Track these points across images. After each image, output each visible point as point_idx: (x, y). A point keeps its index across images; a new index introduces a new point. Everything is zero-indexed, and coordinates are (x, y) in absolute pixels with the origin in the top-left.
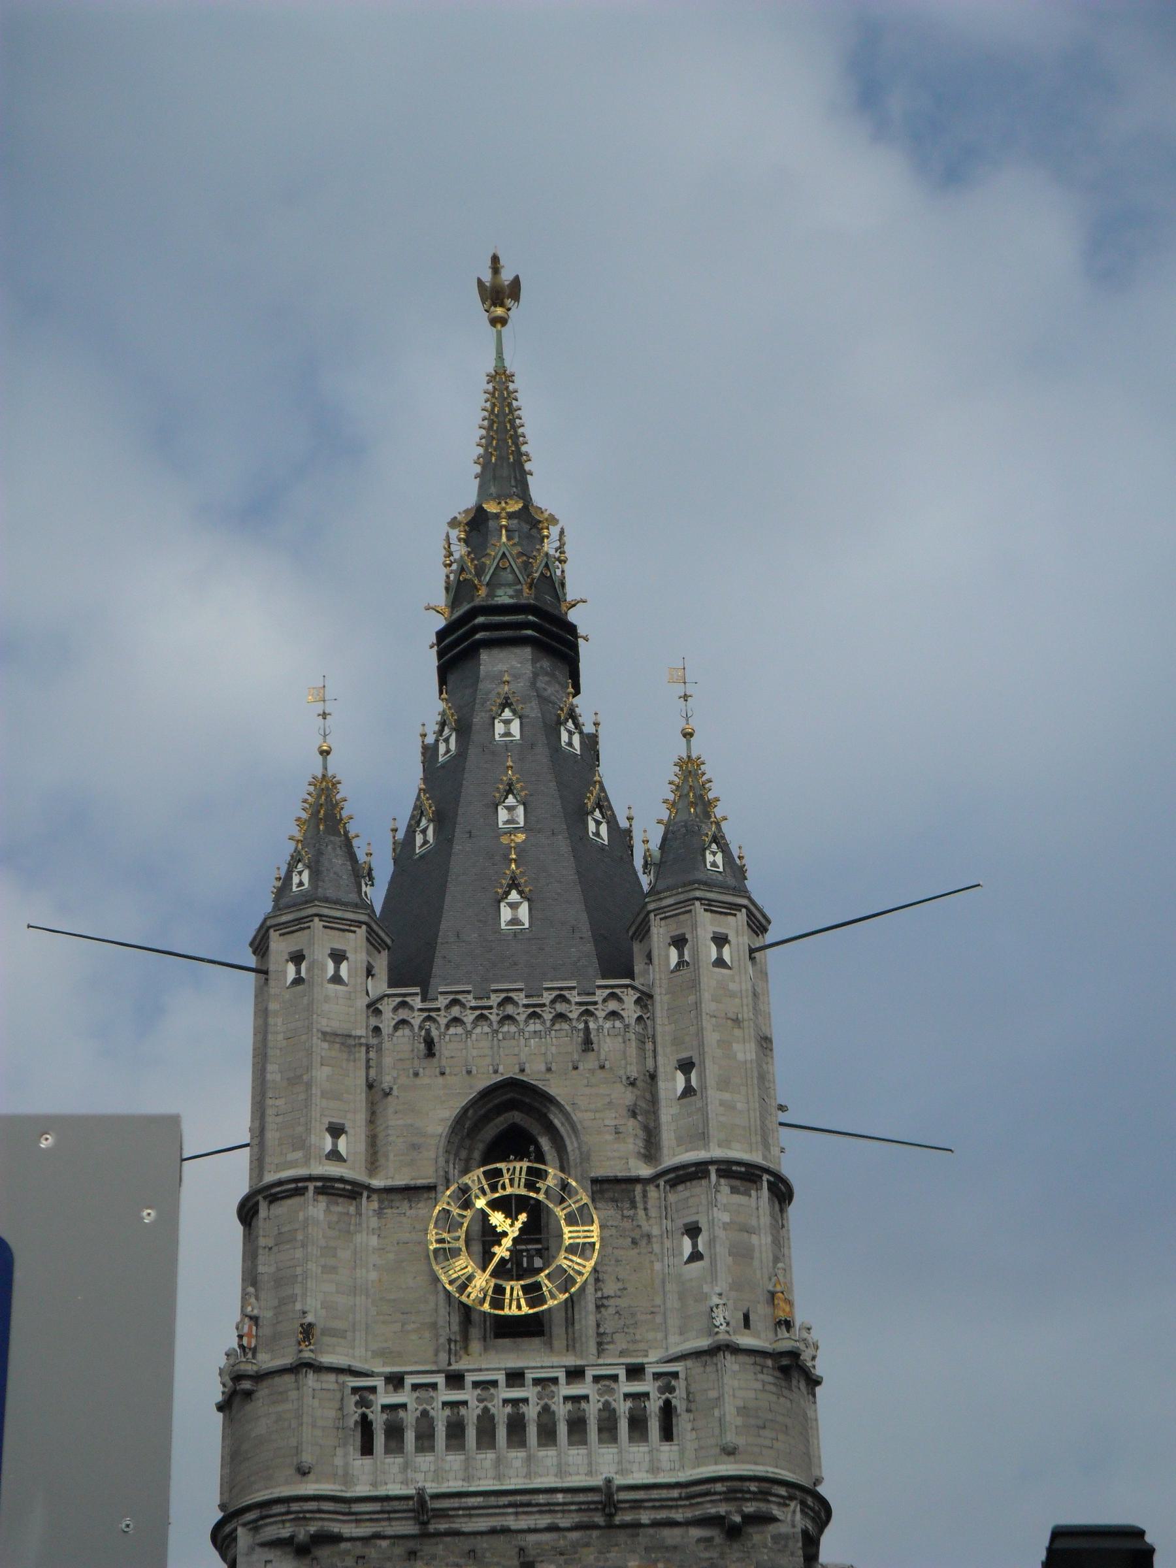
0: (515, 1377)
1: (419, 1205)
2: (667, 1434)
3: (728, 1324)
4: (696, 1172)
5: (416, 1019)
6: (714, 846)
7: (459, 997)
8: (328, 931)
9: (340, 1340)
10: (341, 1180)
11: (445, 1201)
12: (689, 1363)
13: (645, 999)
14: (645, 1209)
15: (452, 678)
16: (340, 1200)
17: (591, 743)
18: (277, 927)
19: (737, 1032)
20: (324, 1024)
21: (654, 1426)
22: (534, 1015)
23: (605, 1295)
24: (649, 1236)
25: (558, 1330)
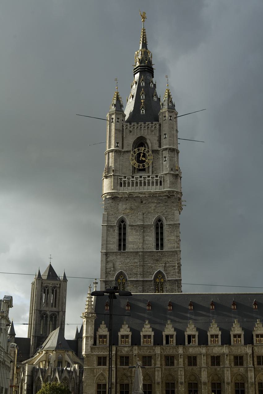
0: (141, 177)
2: (161, 185)
5: (128, 127)
6: (170, 103)
11: (132, 153)
13: (160, 125)
17: (155, 85)
19: (172, 130)
21: (159, 184)
24: (159, 158)
25: (147, 170)
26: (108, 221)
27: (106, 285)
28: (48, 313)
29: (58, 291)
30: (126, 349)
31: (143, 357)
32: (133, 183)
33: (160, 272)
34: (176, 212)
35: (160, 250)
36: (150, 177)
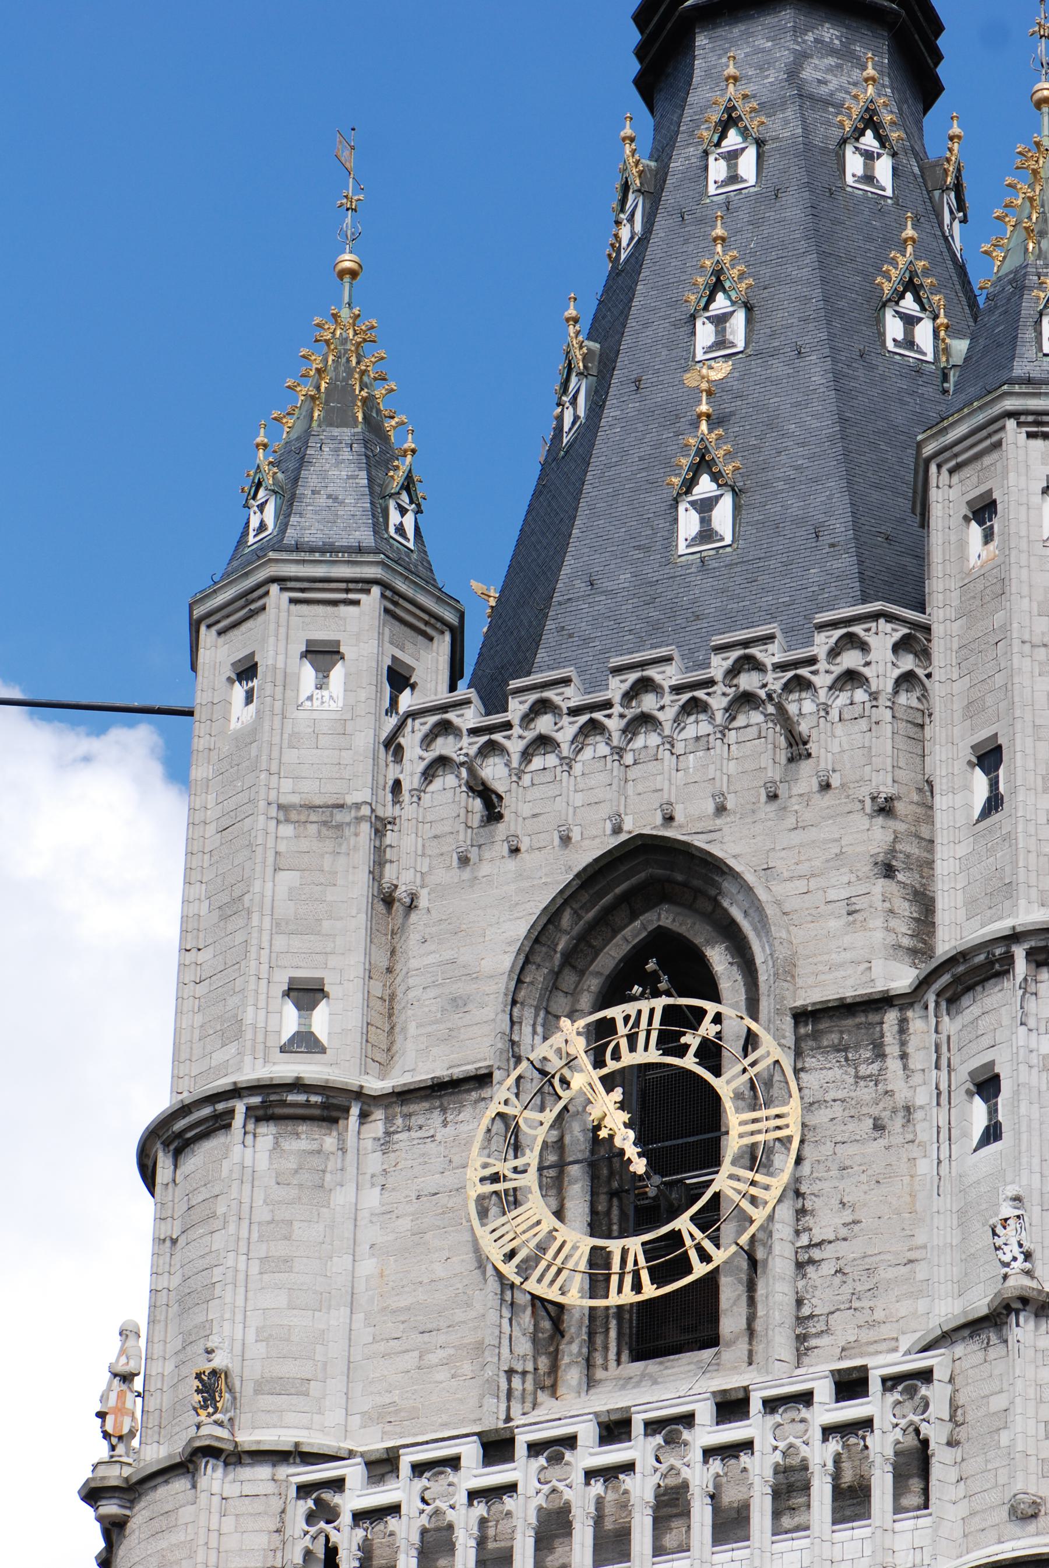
1: (461, 1117)
3: (1028, 1256)
4: (990, 963)
7: (550, 694)
8: (304, 609)
9: (294, 1399)
10: (297, 1085)
12: (959, 1349)
14: (904, 1056)
15: (659, 99)
16: (303, 1128)
18: (210, 618)
20: (288, 791)
22: (694, 707)
23: (815, 1241)
24: (908, 1109)
25: (731, 1322)
36: (756, 1405)
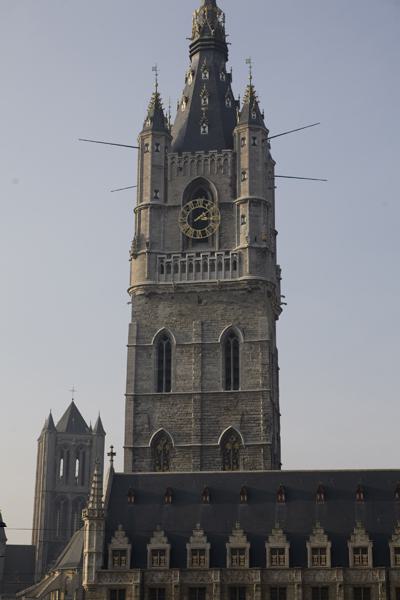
2: (235, 268)
13: (234, 155)
17: (229, 77)
25: (210, 241)
26: (138, 338)
27: (134, 455)
28: (69, 496)
29: (87, 454)
30: (160, 576)
31: (191, 589)
32: (183, 266)
33: (231, 432)
34: (261, 318)
35: (232, 391)
